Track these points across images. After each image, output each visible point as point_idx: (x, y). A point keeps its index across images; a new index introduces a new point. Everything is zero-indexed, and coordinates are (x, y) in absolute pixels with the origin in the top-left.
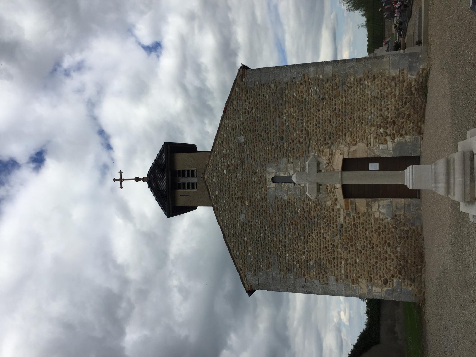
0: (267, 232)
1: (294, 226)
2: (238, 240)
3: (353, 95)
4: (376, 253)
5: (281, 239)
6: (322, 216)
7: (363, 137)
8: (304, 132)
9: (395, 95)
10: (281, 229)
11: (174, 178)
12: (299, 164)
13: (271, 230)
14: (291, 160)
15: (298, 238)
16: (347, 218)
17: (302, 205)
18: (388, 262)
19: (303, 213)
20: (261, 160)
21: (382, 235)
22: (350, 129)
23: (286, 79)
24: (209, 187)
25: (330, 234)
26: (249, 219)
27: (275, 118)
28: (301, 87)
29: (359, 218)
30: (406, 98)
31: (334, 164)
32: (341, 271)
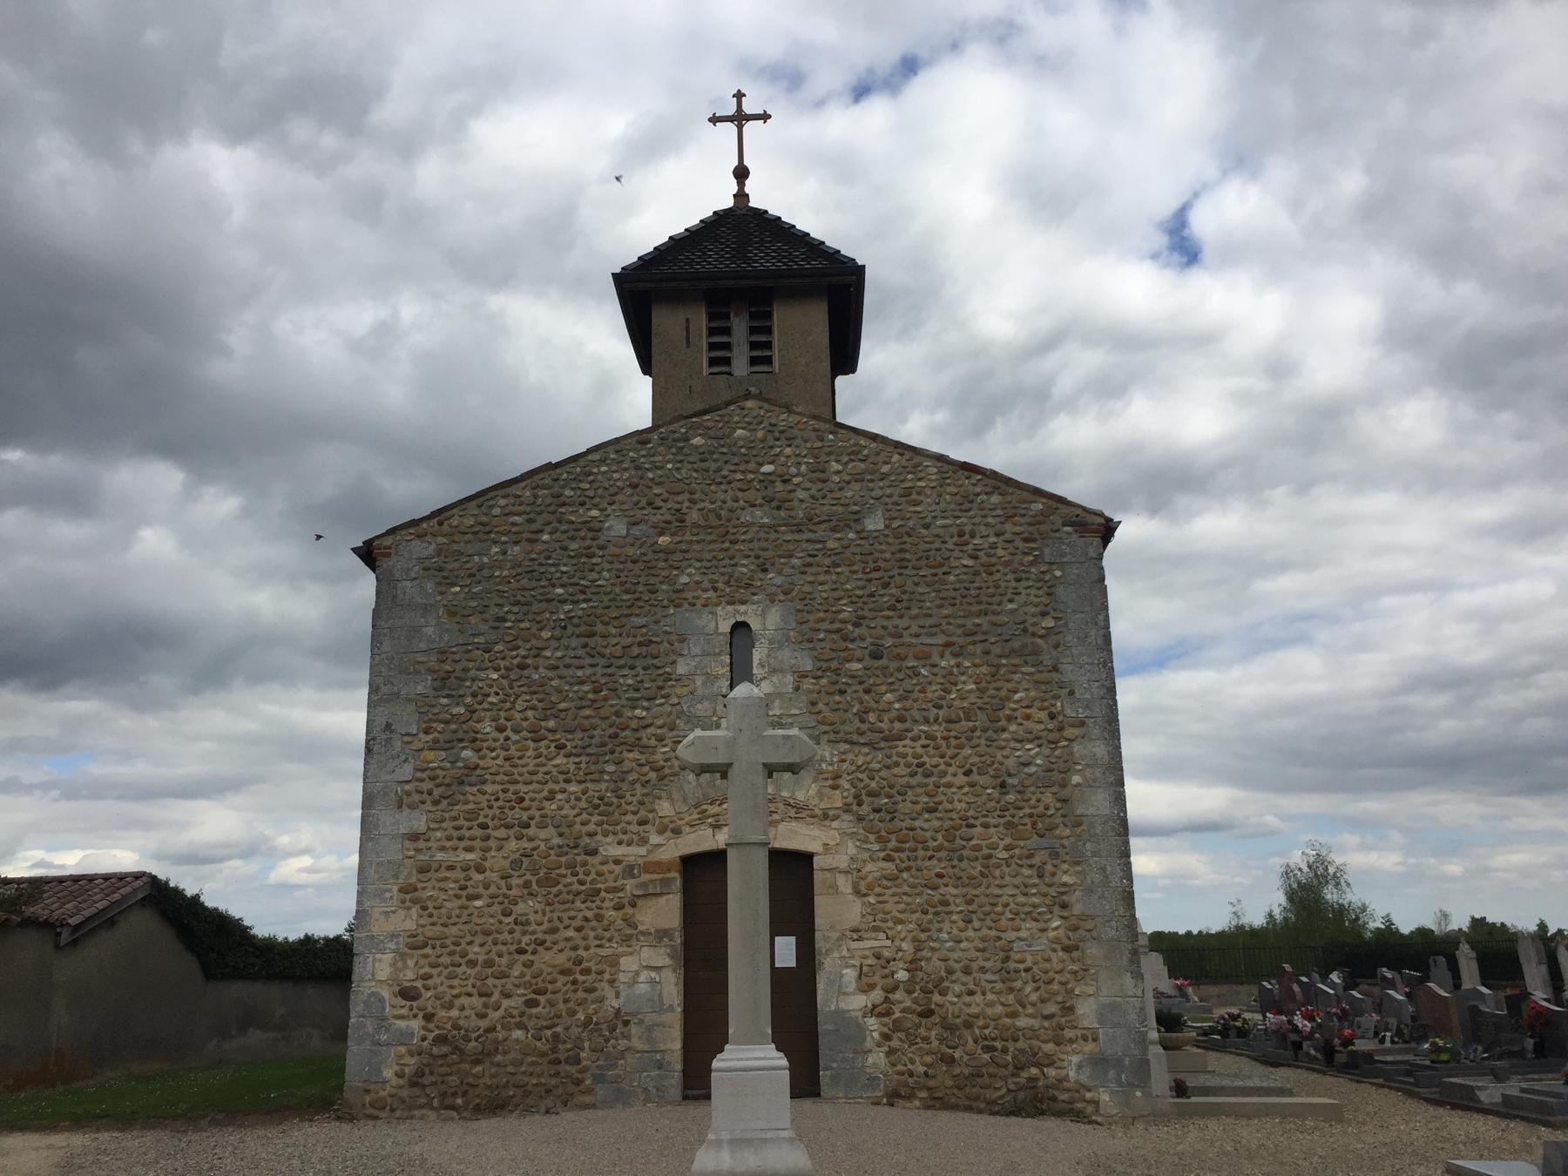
0: (567, 608)
1: (590, 696)
2: (540, 513)
3: (1015, 881)
4: (504, 960)
5: (548, 654)
6: (624, 786)
7: (881, 916)
8: (898, 725)
9: (1014, 1015)
10: (580, 652)
11: (745, 298)
12: (794, 711)
13: (575, 621)
14: (807, 684)
15: (550, 710)
16: (618, 869)
17: (659, 722)
18: (476, 1001)
19: (634, 724)
20: (807, 588)
21: (562, 979)
22: (905, 875)
23: (1070, 667)
24: (715, 416)
25: (564, 812)
26: (612, 550)
27: (943, 632)
28: (1043, 715)
29: (619, 907)
30: (1005, 1051)
31: (794, 824)
32: (443, 849)
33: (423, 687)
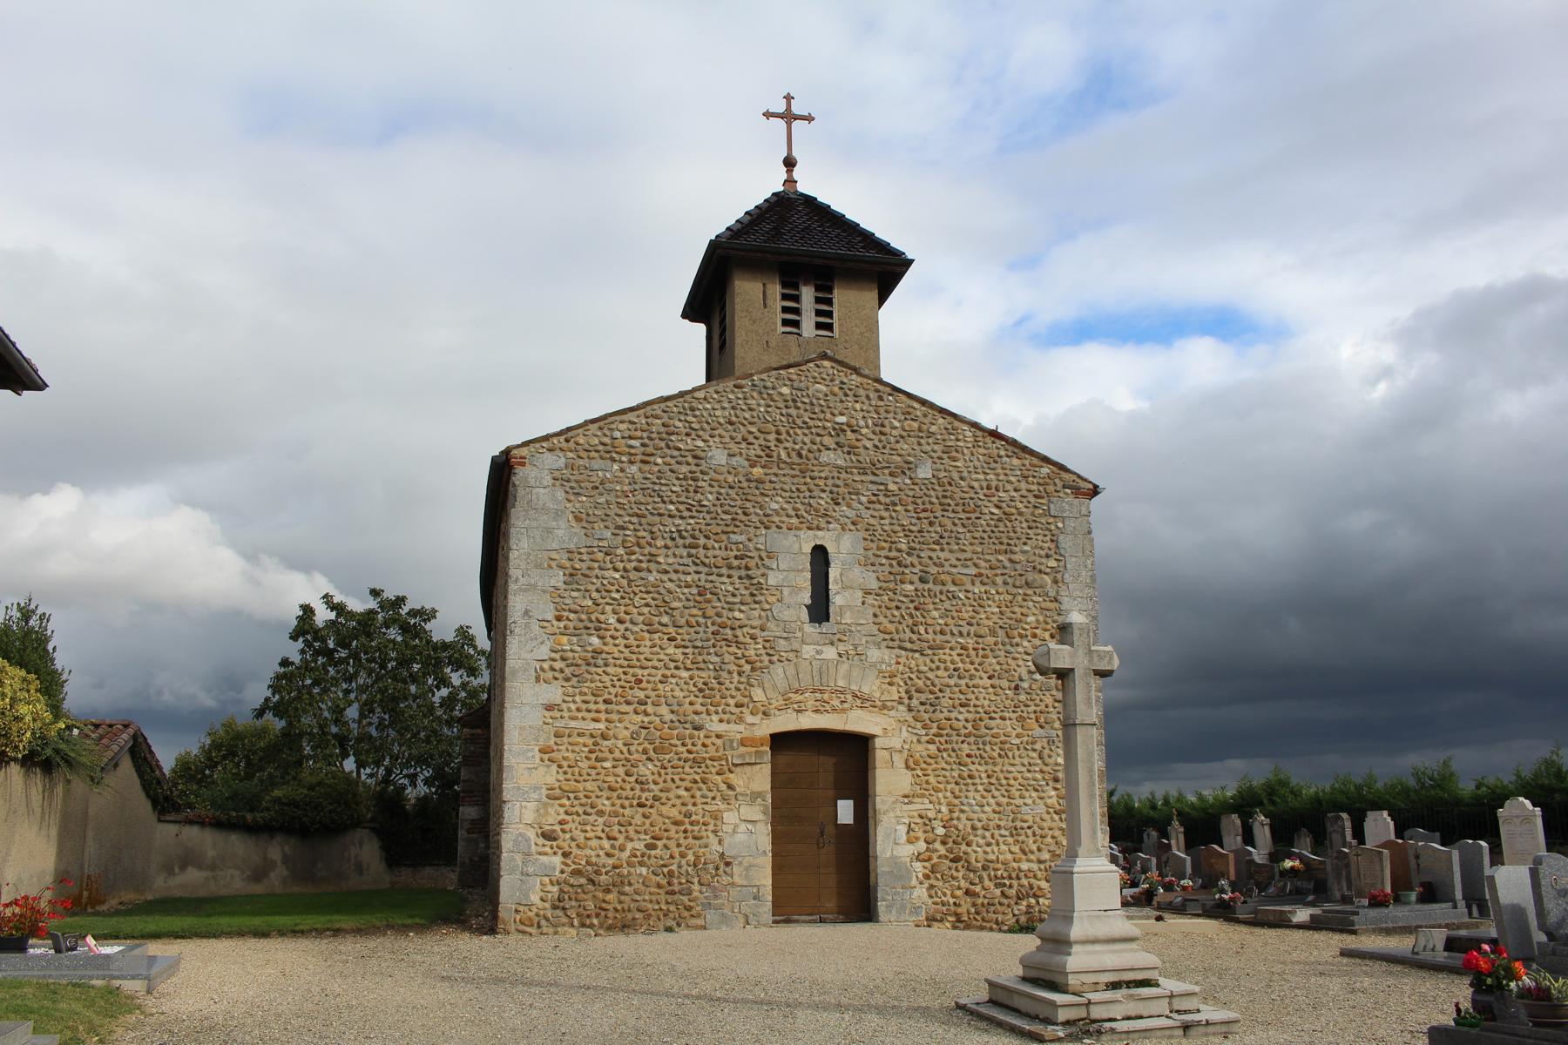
8: (939, 637)
14: (870, 600)
15: (665, 607)
16: (719, 742)
18: (606, 844)
21: (673, 828)
27: (976, 565)
30: (1011, 886)
32: (572, 718)
33: (558, 579)
